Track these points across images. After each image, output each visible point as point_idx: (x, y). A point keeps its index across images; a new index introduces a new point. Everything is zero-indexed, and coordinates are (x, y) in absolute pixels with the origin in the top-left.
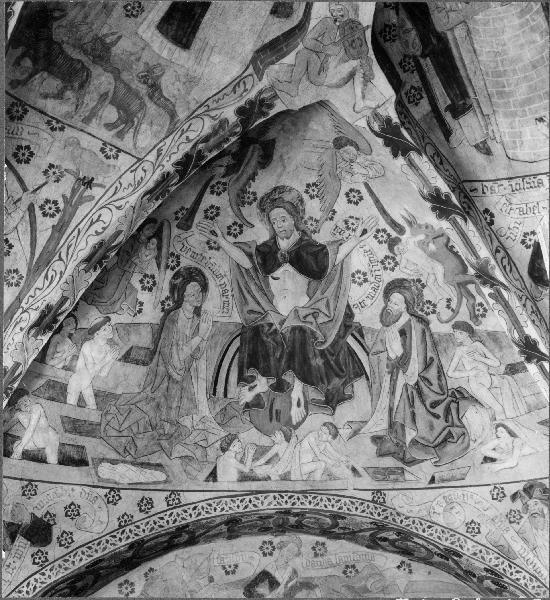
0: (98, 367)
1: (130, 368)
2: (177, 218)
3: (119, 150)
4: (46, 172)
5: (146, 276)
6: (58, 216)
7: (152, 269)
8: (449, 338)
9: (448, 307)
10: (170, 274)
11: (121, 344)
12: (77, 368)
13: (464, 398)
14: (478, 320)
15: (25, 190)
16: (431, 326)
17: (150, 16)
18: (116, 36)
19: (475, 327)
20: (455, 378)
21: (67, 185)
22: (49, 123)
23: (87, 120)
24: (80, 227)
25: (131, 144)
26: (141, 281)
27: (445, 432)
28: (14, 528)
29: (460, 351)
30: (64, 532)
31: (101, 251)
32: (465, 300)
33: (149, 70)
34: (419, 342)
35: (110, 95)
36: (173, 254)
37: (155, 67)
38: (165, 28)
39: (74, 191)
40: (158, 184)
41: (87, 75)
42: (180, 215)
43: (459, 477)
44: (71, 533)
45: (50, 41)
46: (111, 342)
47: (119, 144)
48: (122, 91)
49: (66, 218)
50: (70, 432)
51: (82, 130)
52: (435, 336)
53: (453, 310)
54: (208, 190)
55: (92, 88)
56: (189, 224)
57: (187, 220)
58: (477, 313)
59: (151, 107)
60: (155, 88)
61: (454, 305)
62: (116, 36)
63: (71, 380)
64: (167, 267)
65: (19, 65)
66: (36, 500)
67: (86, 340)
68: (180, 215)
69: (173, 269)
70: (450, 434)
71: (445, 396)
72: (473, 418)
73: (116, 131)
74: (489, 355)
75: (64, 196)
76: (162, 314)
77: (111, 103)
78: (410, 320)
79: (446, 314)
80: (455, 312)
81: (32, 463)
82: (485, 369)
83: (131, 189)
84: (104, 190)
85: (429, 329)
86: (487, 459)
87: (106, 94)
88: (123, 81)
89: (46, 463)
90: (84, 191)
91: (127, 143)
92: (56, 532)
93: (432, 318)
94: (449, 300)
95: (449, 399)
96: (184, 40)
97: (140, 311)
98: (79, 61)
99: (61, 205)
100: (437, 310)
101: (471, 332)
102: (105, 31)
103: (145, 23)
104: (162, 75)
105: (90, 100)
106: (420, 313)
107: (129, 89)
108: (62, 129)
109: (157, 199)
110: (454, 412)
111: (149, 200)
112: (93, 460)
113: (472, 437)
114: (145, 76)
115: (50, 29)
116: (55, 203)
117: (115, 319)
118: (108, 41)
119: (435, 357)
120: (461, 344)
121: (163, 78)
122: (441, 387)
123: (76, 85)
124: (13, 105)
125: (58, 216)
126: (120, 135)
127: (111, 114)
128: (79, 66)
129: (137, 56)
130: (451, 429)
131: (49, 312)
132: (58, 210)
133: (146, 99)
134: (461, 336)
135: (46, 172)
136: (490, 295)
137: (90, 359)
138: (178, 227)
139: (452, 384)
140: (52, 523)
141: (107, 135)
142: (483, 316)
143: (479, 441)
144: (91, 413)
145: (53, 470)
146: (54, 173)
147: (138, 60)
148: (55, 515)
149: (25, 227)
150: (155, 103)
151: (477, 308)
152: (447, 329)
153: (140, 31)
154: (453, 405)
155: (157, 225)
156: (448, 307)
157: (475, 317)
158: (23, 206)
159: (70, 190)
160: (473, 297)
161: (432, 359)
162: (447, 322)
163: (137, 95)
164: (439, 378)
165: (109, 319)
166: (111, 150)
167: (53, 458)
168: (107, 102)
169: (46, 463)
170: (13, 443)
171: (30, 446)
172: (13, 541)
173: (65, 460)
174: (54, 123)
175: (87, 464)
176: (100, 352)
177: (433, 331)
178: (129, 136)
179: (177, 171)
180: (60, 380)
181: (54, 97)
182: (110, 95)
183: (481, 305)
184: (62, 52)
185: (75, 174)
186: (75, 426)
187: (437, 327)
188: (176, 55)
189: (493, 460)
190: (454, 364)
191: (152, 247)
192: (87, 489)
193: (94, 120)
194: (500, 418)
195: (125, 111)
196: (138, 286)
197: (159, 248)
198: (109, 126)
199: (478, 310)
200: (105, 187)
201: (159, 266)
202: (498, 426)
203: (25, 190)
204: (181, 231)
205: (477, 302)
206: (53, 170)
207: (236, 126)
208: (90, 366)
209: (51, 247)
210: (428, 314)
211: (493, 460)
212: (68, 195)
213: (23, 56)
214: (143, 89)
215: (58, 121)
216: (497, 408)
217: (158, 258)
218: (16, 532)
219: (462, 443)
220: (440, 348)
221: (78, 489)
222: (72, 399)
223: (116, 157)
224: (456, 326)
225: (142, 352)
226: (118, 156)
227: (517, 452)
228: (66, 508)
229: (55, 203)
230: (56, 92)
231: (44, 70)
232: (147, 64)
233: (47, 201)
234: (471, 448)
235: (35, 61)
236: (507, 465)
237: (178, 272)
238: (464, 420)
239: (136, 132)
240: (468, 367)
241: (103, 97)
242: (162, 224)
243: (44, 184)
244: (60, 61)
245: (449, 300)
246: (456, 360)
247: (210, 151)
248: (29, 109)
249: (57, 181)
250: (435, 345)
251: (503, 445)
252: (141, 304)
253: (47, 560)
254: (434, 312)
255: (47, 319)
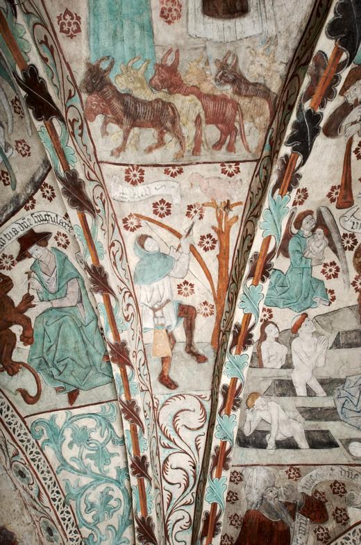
0: (313, 360)
1: (345, 353)
2: (332, 200)
3: (237, 163)
4: (188, 214)
5: (325, 265)
6: (217, 246)
7: (330, 257)
10: (350, 255)
11: (327, 334)
12: (295, 364)
15: (179, 236)
17: (191, 6)
18: (173, 53)
21: (210, 216)
22: (167, 172)
23: (196, 151)
24: (237, 248)
25: (244, 151)
26: (323, 272)
28: (291, 508)
30: (337, 509)
31: (260, 263)
33: (223, 66)
35: (202, 116)
36: (345, 235)
37: (226, 58)
38: (211, 7)
39: (219, 220)
40: (282, 175)
41: (172, 108)
42: (334, 196)
44: (344, 510)
45: (120, 96)
46: (316, 334)
47: (234, 157)
48: (211, 105)
49: (224, 244)
50: (310, 420)
51: (197, 163)
54: (353, 156)
55: (183, 119)
56: (349, 199)
57: (345, 197)
59: (244, 102)
60: (238, 80)
62: (173, 53)
63: (292, 375)
64: (345, 249)
65: (107, 134)
66: (303, 481)
67: (292, 339)
68: (334, 196)
69: (351, 249)
73: (224, 147)
75: (213, 228)
76: (358, 293)
77: (207, 123)
81: (287, 450)
83: (260, 192)
84: (242, 207)
87: (199, 116)
88: (208, 96)
89: (300, 449)
90: (227, 215)
91: (240, 153)
92: (330, 509)
96: (238, 8)
97: (334, 299)
98: (157, 100)
99: (215, 236)
102: (160, 55)
103: (190, 17)
104: (237, 61)
105: (189, 130)
107: (214, 98)
108: (180, 171)
109: (290, 189)
111: (282, 194)
112: (341, 441)
114: (223, 74)
115: (111, 85)
116: (209, 236)
117: (312, 313)
118: (169, 63)
121: (240, 65)
123: (169, 125)
124: (127, 172)
125: (217, 246)
126: (231, 148)
127: (212, 133)
128: (160, 105)
129: (204, 60)
131: (239, 331)
132: (214, 241)
133: (236, 97)
135: (188, 214)
137: (303, 355)
138: (339, 207)
140: (323, 500)
141: (222, 155)
144: (323, 401)
145: (307, 454)
146: (195, 212)
147: (207, 63)
148: (324, 493)
149: (195, 267)
150: (246, 96)
153: (192, 32)
155: (315, 216)
158: (186, 248)
159: (215, 219)
163: (224, 99)
165: (306, 315)
166: (230, 166)
167: (303, 444)
168: (204, 125)
169: (300, 449)
170: (265, 436)
171: (280, 437)
172: (294, 518)
173: (314, 444)
174: (171, 169)
175: (337, 446)
176: (310, 346)
178: (239, 145)
179: (294, 149)
180: (283, 378)
181: (157, 147)
182: (202, 116)
184: (136, 100)
185: (213, 204)
186: (312, 414)
188: (239, 29)
191: (319, 237)
192: (346, 468)
193: (202, 148)
195: (223, 122)
196: (323, 277)
197: (328, 235)
198: (218, 145)
200: (241, 203)
201: (335, 251)
203: (179, 236)
204: (344, 211)
206: (193, 210)
207: (338, 54)
208: (305, 360)
209: (224, 274)
212: (216, 224)
213: (105, 123)
214: (228, 90)
215: (174, 166)
217: (331, 245)
218: (295, 510)
221: (337, 469)
222: (301, 391)
223: (238, 171)
225: (353, 335)
226: (238, 168)
228: (331, 486)
229: (209, 236)
230: (156, 141)
231: (133, 126)
232: (217, 61)
233: (203, 238)
235: (119, 122)
237: (359, 247)
239: (243, 137)
241: (198, 121)
242: (320, 213)
243: (192, 225)
244: (141, 110)
247: (322, 105)
248: (143, 168)
249: (201, 217)
252: (332, 292)
253: (329, 537)
255: (240, 338)
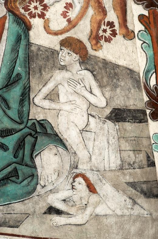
8: (53, 54)
9: (64, 15)
13: (46, 134)
14: (97, 42)
16: (31, 33)
19: (91, 52)
20: (40, 108)
27: (9, 169)
29: (59, 76)
32: (91, 11)
34: (9, 48)
43: (11, 223)
52: (33, 48)
53: (69, 21)
58: (101, 33)
61: (73, 14)
70: (15, 170)
71: (22, 126)
72: (48, 161)
74: (96, 90)
78: (4, 17)
79: (58, 22)
80: (72, 24)
82: (85, 107)
85: (27, 36)
86: (52, 210)
93: (37, 22)
94: (69, 6)
95: (26, 130)
100: (48, 15)
101: (85, 59)
106: (22, 11)
110: (28, 147)
113: (42, 183)
119: (23, 74)
120: (63, 68)
122: (20, 113)
130: (18, 167)
134: (68, 57)
136: (141, 18)
139: (36, 114)
142: (108, 40)
143: (49, 188)
151: (103, 27)
152: (53, 42)
154: (29, 140)
156: (64, 15)
157: (96, 38)
160: (104, 12)
161: (18, 75)
162: (56, 34)
164: (22, 102)
177: (32, 41)
183: (111, 24)
187: (39, 37)
189: (59, 212)
190: (45, 90)
194: (83, 168)
199: (105, 31)
202: (77, 176)
205: (106, 21)
210: (33, 16)
211: (59, 212)
216: (82, 154)
219: (28, 184)
220: (33, 65)
224: (64, 43)
227: (89, 211)
234: (34, 194)
236: (73, 220)
238: (37, 161)
240: (62, 98)
245: (69, 6)
246: (51, 85)
250: (29, 59)
251: (76, 198)
254: (42, 16)
